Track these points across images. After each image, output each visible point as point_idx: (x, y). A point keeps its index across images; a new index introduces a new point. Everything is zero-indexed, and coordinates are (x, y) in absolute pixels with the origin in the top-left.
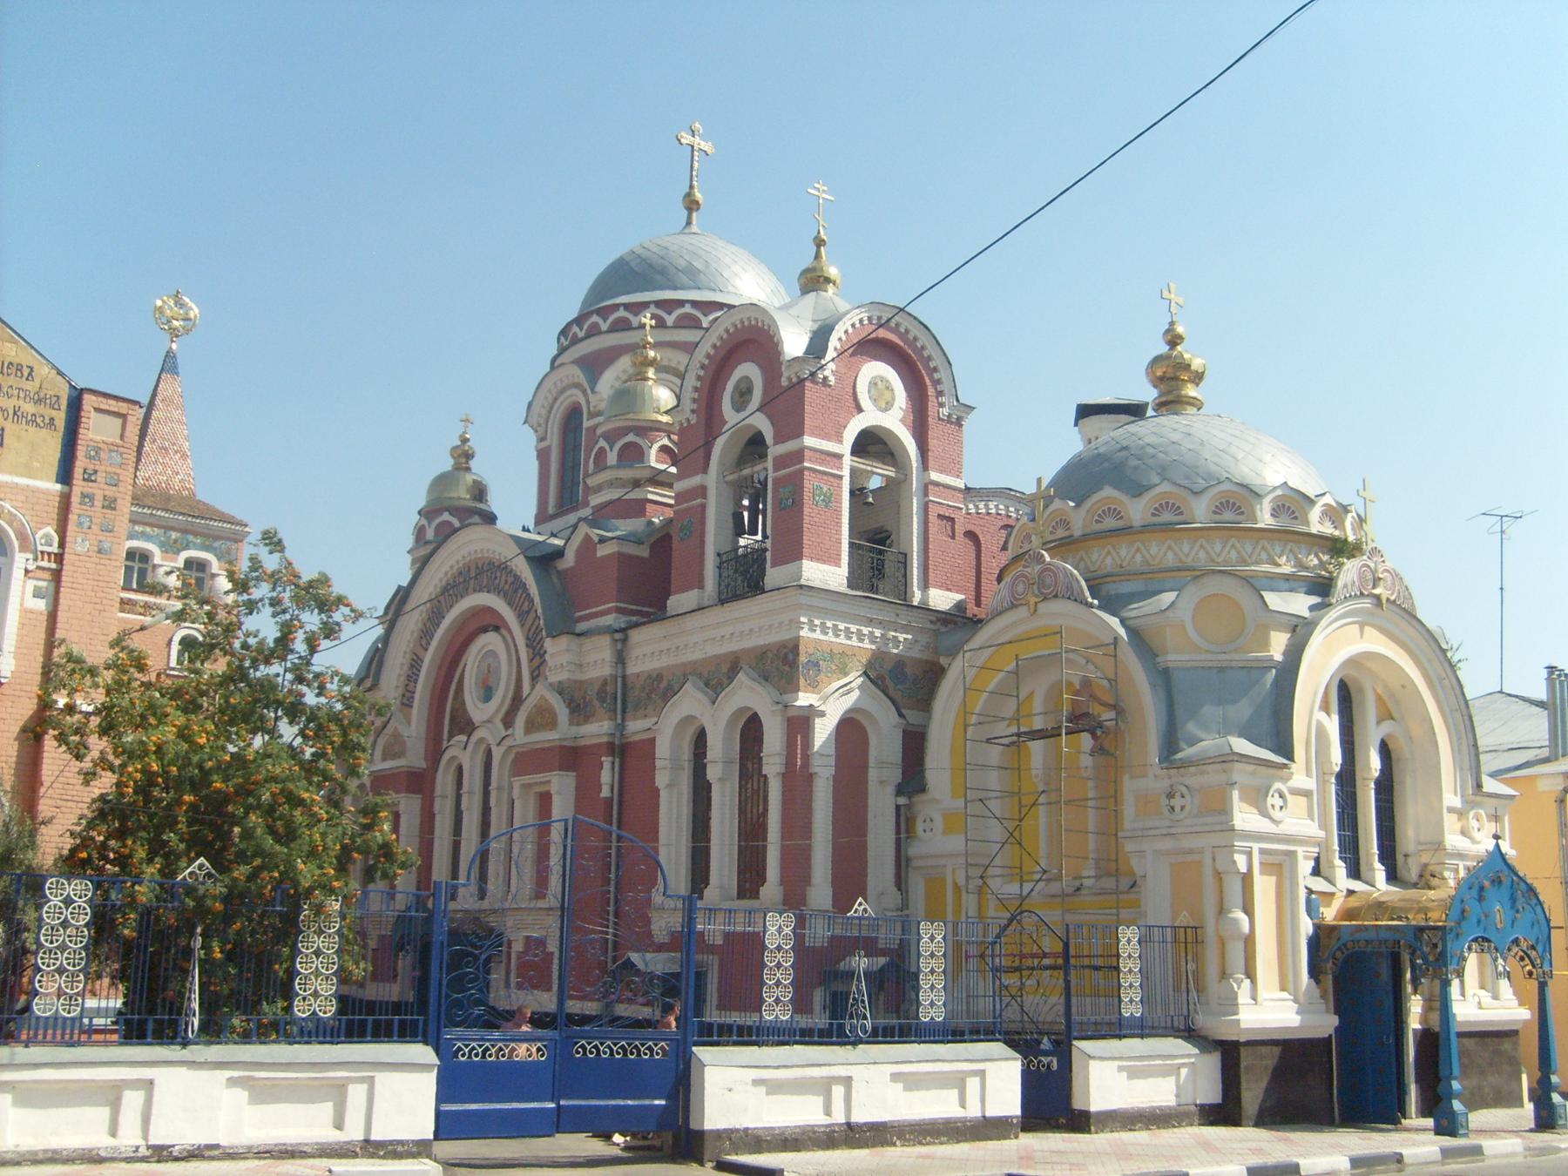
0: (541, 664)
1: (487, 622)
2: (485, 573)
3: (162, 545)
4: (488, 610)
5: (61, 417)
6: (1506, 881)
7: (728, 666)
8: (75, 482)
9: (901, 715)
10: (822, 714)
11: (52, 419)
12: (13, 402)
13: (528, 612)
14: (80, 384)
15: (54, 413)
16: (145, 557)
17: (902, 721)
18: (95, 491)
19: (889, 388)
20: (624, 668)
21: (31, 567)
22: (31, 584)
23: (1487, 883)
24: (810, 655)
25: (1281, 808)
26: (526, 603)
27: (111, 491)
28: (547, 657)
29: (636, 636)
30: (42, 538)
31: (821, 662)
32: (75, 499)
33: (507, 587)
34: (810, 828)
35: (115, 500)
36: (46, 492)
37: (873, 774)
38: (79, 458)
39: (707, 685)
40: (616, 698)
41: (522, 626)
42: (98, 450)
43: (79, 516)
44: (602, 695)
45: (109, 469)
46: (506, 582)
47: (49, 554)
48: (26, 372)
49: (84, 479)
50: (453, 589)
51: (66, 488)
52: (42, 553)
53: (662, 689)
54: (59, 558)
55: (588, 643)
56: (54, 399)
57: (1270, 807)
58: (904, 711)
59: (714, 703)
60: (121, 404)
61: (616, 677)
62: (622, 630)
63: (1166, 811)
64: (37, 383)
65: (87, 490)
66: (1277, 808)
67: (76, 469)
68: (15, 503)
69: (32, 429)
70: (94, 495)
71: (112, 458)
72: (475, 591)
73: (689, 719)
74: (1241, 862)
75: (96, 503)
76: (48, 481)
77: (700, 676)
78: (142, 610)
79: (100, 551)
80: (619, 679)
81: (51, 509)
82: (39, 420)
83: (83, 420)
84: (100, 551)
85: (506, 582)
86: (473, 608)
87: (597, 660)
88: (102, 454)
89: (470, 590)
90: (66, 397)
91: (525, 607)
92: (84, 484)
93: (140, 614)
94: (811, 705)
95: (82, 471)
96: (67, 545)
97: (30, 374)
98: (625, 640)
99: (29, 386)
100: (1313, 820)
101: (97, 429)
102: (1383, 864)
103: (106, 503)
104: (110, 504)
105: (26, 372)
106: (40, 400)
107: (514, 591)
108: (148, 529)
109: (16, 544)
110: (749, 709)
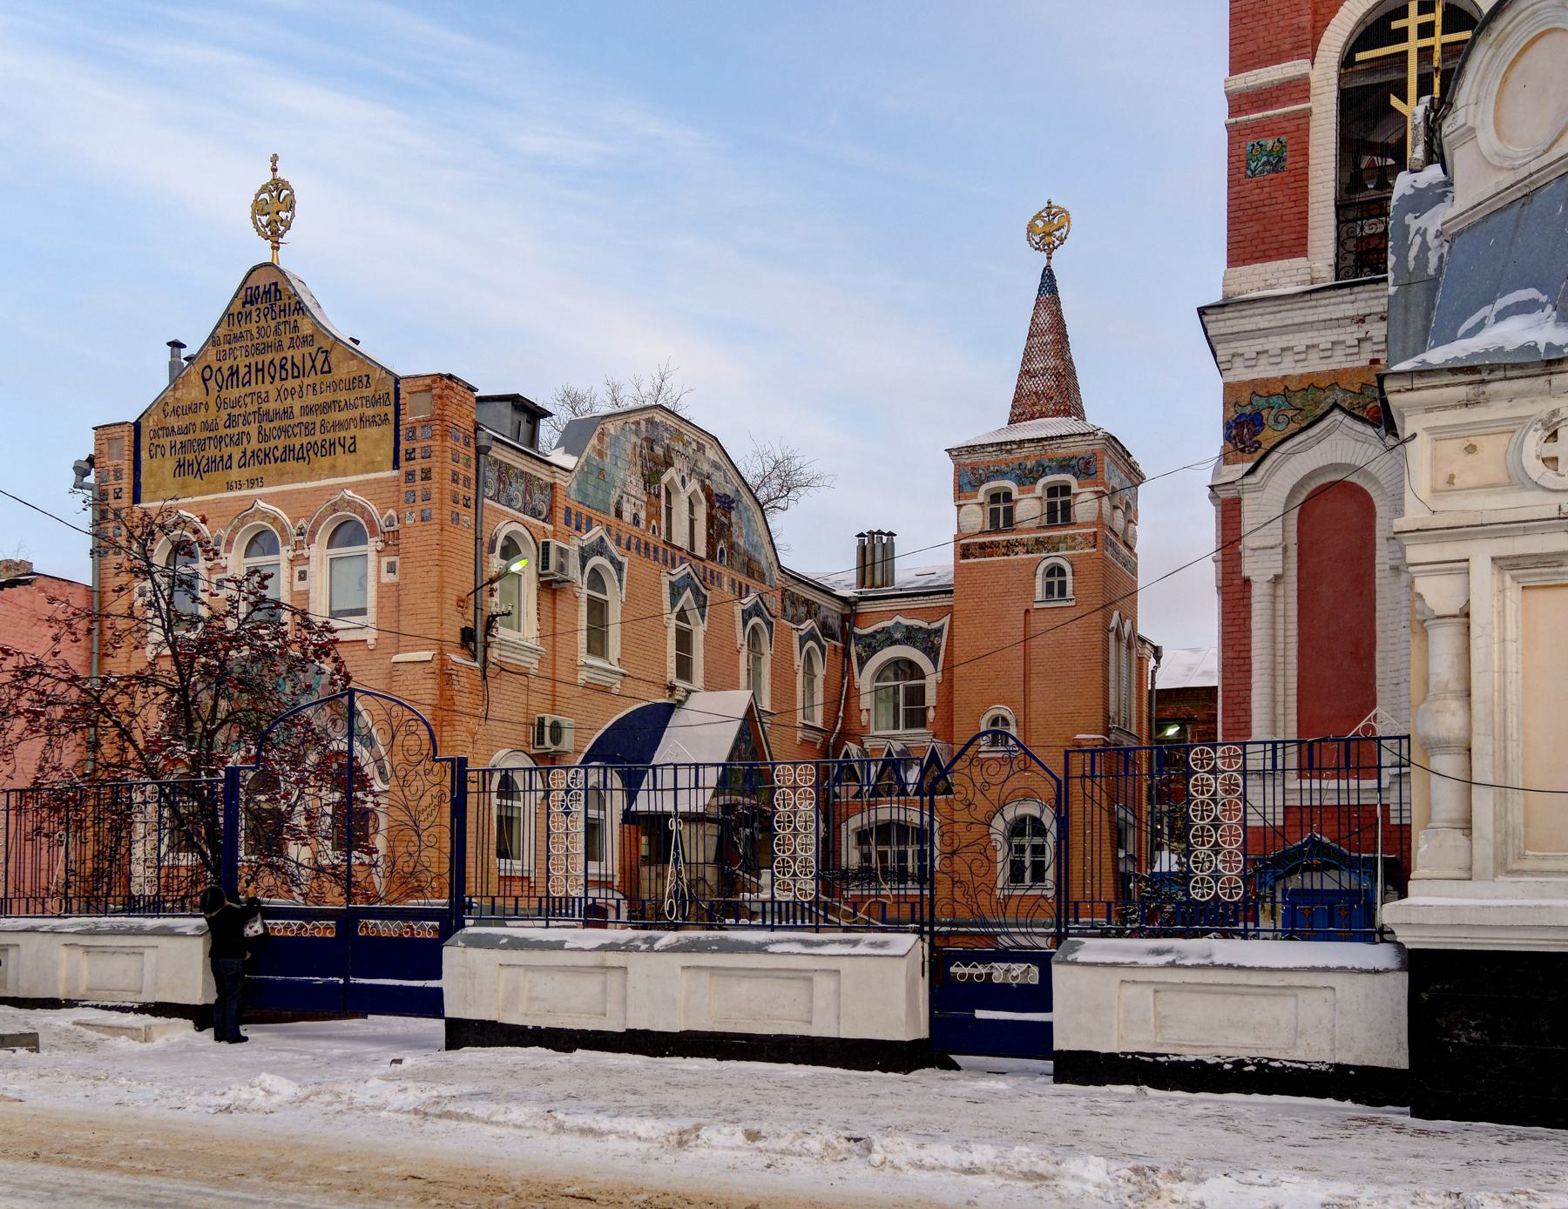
5: (390, 410)
10: (1259, 488)
12: (360, 410)
16: (1008, 496)
27: (425, 464)
31: (1263, 413)
34: (1250, 658)
36: (387, 480)
45: (424, 444)
48: (365, 380)
64: (373, 388)
65: (410, 469)
78: (1004, 551)
79: (423, 520)
84: (423, 520)
93: (1004, 555)
99: (368, 392)
104: (427, 474)
105: (365, 380)
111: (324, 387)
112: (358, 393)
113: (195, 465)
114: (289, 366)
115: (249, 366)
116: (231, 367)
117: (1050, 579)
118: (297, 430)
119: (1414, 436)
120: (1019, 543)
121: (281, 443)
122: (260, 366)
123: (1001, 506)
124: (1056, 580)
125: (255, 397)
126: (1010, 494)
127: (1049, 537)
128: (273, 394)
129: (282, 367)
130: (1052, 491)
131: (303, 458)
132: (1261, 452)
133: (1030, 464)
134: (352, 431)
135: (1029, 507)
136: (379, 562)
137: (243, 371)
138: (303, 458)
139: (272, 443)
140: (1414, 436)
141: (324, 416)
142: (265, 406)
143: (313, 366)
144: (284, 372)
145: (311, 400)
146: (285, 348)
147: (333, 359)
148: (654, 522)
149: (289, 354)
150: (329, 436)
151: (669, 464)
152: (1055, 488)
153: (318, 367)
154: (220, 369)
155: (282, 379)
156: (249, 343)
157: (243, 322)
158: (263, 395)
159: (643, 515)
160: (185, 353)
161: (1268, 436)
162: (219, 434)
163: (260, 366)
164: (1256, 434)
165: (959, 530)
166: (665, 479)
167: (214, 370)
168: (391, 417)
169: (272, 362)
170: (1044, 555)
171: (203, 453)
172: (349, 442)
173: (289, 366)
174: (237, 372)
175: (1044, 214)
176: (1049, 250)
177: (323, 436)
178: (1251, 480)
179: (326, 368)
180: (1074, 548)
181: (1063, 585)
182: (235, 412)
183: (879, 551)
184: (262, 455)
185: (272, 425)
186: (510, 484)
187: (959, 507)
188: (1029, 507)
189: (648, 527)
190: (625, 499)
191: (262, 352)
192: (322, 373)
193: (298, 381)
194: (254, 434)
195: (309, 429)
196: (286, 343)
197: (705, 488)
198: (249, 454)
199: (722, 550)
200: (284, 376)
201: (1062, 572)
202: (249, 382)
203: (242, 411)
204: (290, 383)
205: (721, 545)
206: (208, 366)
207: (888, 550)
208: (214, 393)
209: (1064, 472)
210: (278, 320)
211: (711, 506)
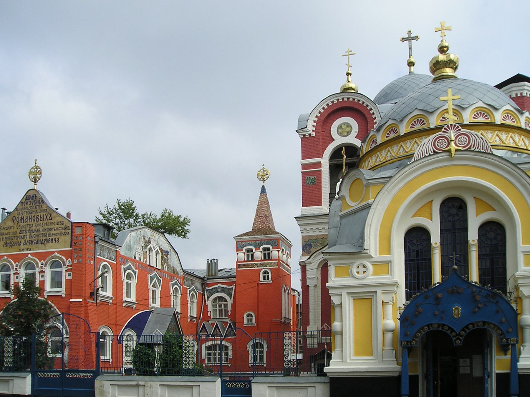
3: (255, 246)
5: (70, 231)
8: (73, 246)
11: (68, 232)
15: (68, 231)
19: (340, 127)
24: (307, 242)
25: (364, 272)
48: (62, 222)
49: (75, 245)
64: (64, 225)
66: (361, 272)
76: (68, 248)
78: (251, 266)
82: (66, 233)
93: (251, 267)
97: (63, 223)
105: (62, 222)
108: (250, 242)
109: (36, 266)
111: (50, 224)
112: (60, 226)
113: (10, 243)
114: (39, 218)
115: (27, 217)
116: (22, 217)
117: (265, 275)
118: (41, 235)
119: (330, 265)
120: (256, 264)
123: (250, 253)
124: (266, 275)
125: (29, 226)
126: (252, 250)
127: (264, 263)
128: (34, 225)
129: (37, 218)
130: (265, 249)
132: (311, 253)
133: (258, 242)
134: (58, 236)
135: (259, 254)
139: (34, 239)
140: (330, 265)
141: (49, 232)
143: (47, 218)
144: (38, 219)
145: (46, 227)
148: (145, 259)
149: (39, 214)
151: (150, 243)
152: (266, 249)
154: (18, 218)
155: (37, 221)
156: (27, 210)
158: (31, 225)
159: (142, 258)
160: (6, 211)
161: (313, 250)
162: (17, 235)
163: (30, 217)
164: (310, 249)
165: (237, 260)
166: (149, 247)
167: (16, 217)
168: (70, 233)
169: (34, 216)
170: (263, 268)
171: (12, 241)
172: (57, 239)
173: (39, 218)
174: (23, 218)
175: (262, 170)
176: (264, 180)
177: (49, 238)
178: (309, 260)
179: (50, 219)
180: (271, 266)
181: (268, 276)
182: (23, 229)
183: (214, 265)
184: (30, 242)
185: (34, 234)
186: (104, 251)
187: (237, 253)
188: (259, 254)
189: (143, 261)
190: (137, 253)
191: (31, 213)
192: (49, 220)
193: (42, 222)
194: (28, 236)
195: (45, 235)
197: (160, 249)
198: (26, 242)
199: (166, 267)
200: (38, 220)
201: (268, 273)
202: (27, 221)
203: (24, 229)
204: (39, 222)
205: (165, 265)
206: (14, 216)
207: (216, 264)
208: (16, 224)
209: (268, 244)
211: (162, 254)
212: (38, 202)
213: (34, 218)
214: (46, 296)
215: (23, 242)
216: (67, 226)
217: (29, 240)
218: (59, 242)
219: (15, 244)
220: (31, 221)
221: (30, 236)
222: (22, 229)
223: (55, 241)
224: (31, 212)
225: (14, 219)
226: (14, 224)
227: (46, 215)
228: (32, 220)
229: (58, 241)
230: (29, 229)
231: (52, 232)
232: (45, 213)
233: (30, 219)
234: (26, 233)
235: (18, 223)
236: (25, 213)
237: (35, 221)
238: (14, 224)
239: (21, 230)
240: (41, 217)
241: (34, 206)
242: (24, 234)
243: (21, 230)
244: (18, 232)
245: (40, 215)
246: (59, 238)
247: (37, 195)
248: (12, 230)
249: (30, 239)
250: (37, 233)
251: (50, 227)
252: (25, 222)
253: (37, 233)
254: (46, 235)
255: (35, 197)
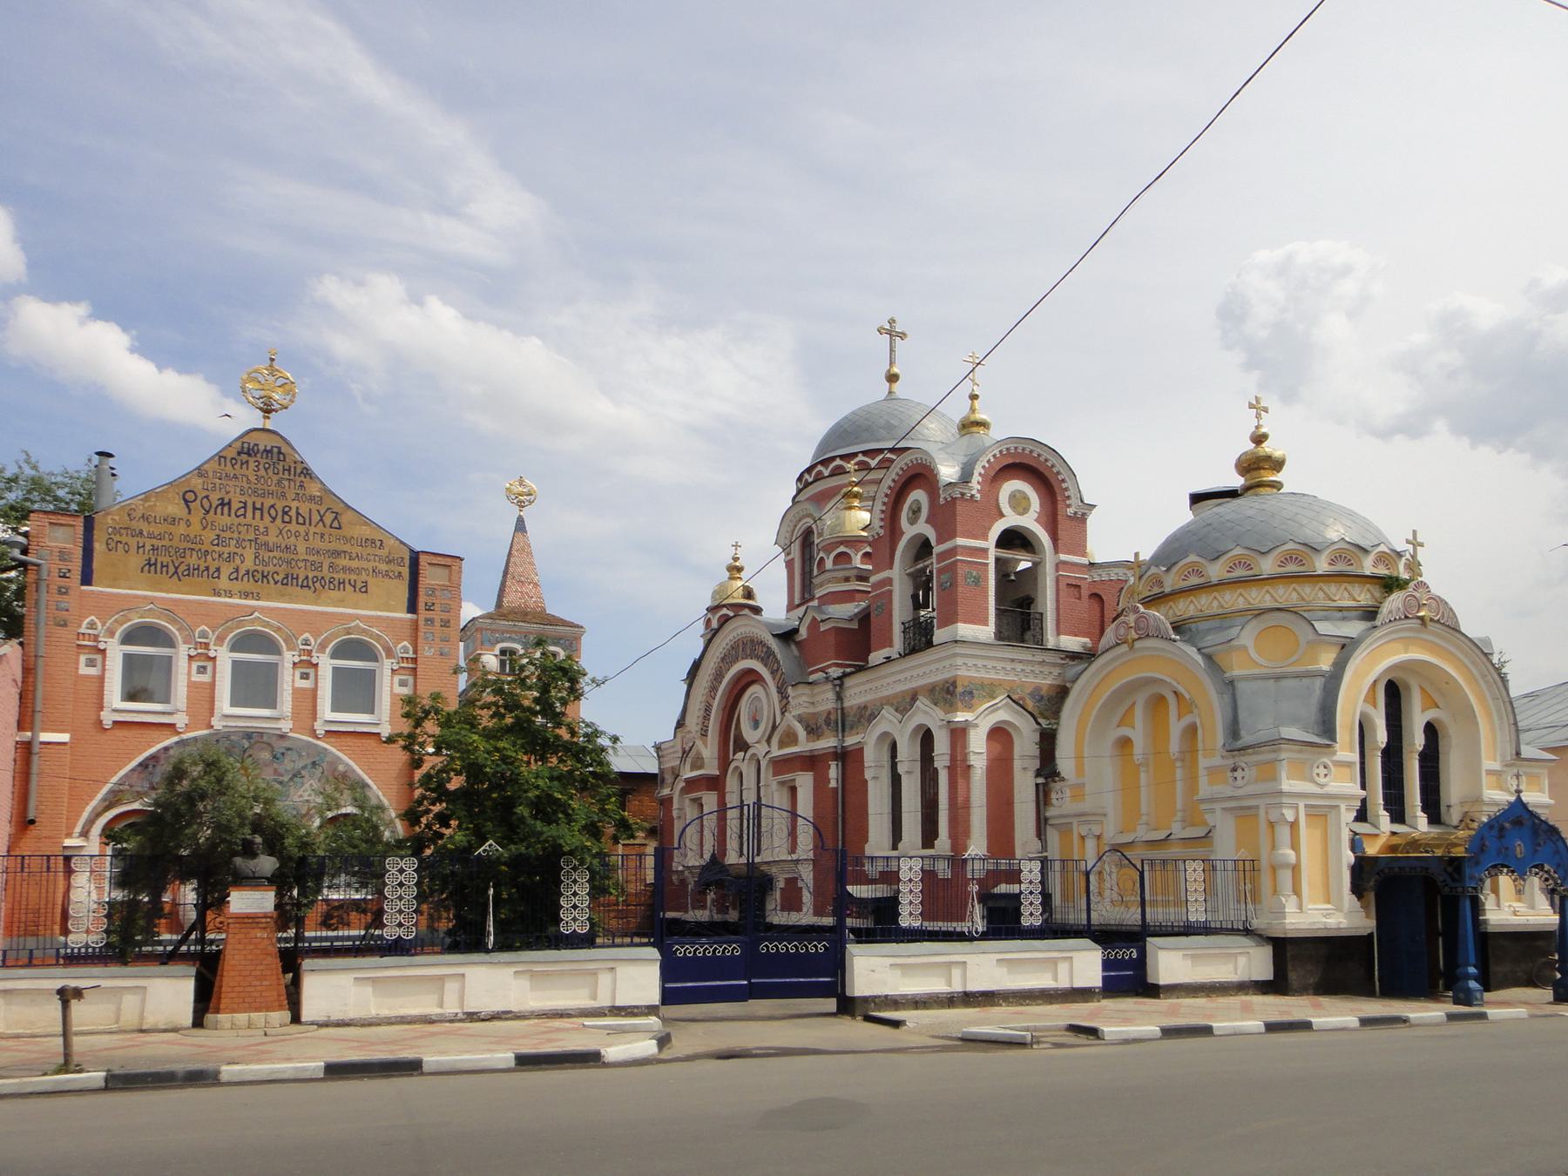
0: (787, 704)
1: (748, 678)
2: (750, 646)
4: (751, 671)
5: (406, 571)
6: (1528, 823)
7: (910, 697)
8: (420, 612)
9: (1038, 723)
12: (372, 564)
13: (777, 670)
14: (418, 548)
15: (401, 569)
17: (1038, 727)
18: (435, 617)
20: (842, 703)
21: (395, 668)
22: (397, 679)
23: (1507, 825)
25: (1326, 775)
26: (776, 665)
27: (445, 616)
28: (790, 699)
29: (848, 682)
30: (400, 649)
32: (421, 623)
33: (763, 655)
35: (449, 621)
36: (400, 620)
37: (1017, 764)
38: (421, 596)
39: (896, 711)
40: (837, 723)
41: (774, 679)
42: (434, 590)
43: (425, 633)
44: (827, 722)
46: (762, 651)
47: (407, 658)
48: (378, 544)
50: (728, 659)
51: (414, 616)
52: (402, 658)
53: (867, 715)
54: (415, 660)
55: (817, 689)
56: (399, 560)
57: (1315, 775)
58: (1040, 720)
59: (900, 722)
60: (446, 559)
61: (837, 709)
62: (839, 678)
63: (1231, 780)
65: (428, 616)
67: (420, 604)
68: (380, 628)
69: (387, 580)
70: (433, 619)
71: (444, 594)
72: (742, 659)
73: (885, 735)
74: (1289, 815)
75: (436, 624)
77: (892, 705)
80: (839, 711)
81: (405, 630)
83: (421, 571)
84: (441, 654)
85: (762, 651)
86: (742, 670)
87: (825, 700)
88: (437, 592)
89: (740, 658)
90: (408, 558)
91: (775, 668)
92: (427, 612)
94: (967, 720)
95: (424, 604)
96: (419, 652)
97: (381, 545)
98: (841, 686)
99: (384, 552)
100: (1355, 783)
101: (430, 577)
102: (1425, 813)
103: (443, 624)
105: (378, 544)
106: (390, 561)
107: (768, 657)
110: (925, 725)
112: (369, 550)
114: (293, 513)
115: (245, 503)
116: (222, 499)
118: (302, 564)
121: (283, 570)
122: (258, 506)
128: (273, 531)
129: (285, 513)
131: (308, 586)
134: (364, 577)
136: (392, 680)
137: (235, 505)
138: (308, 586)
139: (271, 568)
142: (262, 538)
145: (317, 544)
146: (289, 500)
147: (344, 519)
149: (294, 505)
150: (341, 576)
153: (328, 522)
154: (207, 497)
157: (237, 467)
158: (262, 530)
162: (204, 548)
169: (272, 506)
172: (359, 585)
173: (293, 513)
174: (229, 503)
179: (336, 524)
182: (228, 534)
185: (271, 554)
192: (331, 527)
196: (291, 495)
202: (244, 515)
204: (293, 527)
210: (281, 475)
212: (289, 470)
213: (273, 512)
214: (320, 732)
215: (226, 570)
216: (396, 556)
217: (252, 570)
218: (366, 592)
219: (190, 571)
220: (262, 519)
221: (256, 557)
222: (223, 535)
223: (354, 587)
224: (260, 492)
225: (190, 497)
226: (190, 513)
227: (318, 511)
228: (266, 515)
229: (364, 589)
230: (252, 537)
231: (343, 562)
232: (314, 507)
233: (258, 513)
234: (239, 543)
235: (208, 512)
236: (238, 490)
237: (279, 520)
238: (190, 513)
239: (218, 536)
240: (298, 513)
241: (275, 478)
242: (232, 549)
243: (218, 536)
244: (210, 535)
245: (297, 508)
246: (366, 582)
247: (282, 451)
248: (181, 529)
249: (260, 568)
250: (285, 556)
251: (334, 546)
252: (238, 517)
253: (285, 556)
254: (321, 567)
255: (275, 456)
